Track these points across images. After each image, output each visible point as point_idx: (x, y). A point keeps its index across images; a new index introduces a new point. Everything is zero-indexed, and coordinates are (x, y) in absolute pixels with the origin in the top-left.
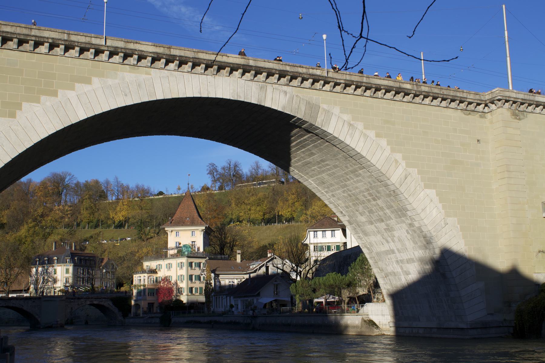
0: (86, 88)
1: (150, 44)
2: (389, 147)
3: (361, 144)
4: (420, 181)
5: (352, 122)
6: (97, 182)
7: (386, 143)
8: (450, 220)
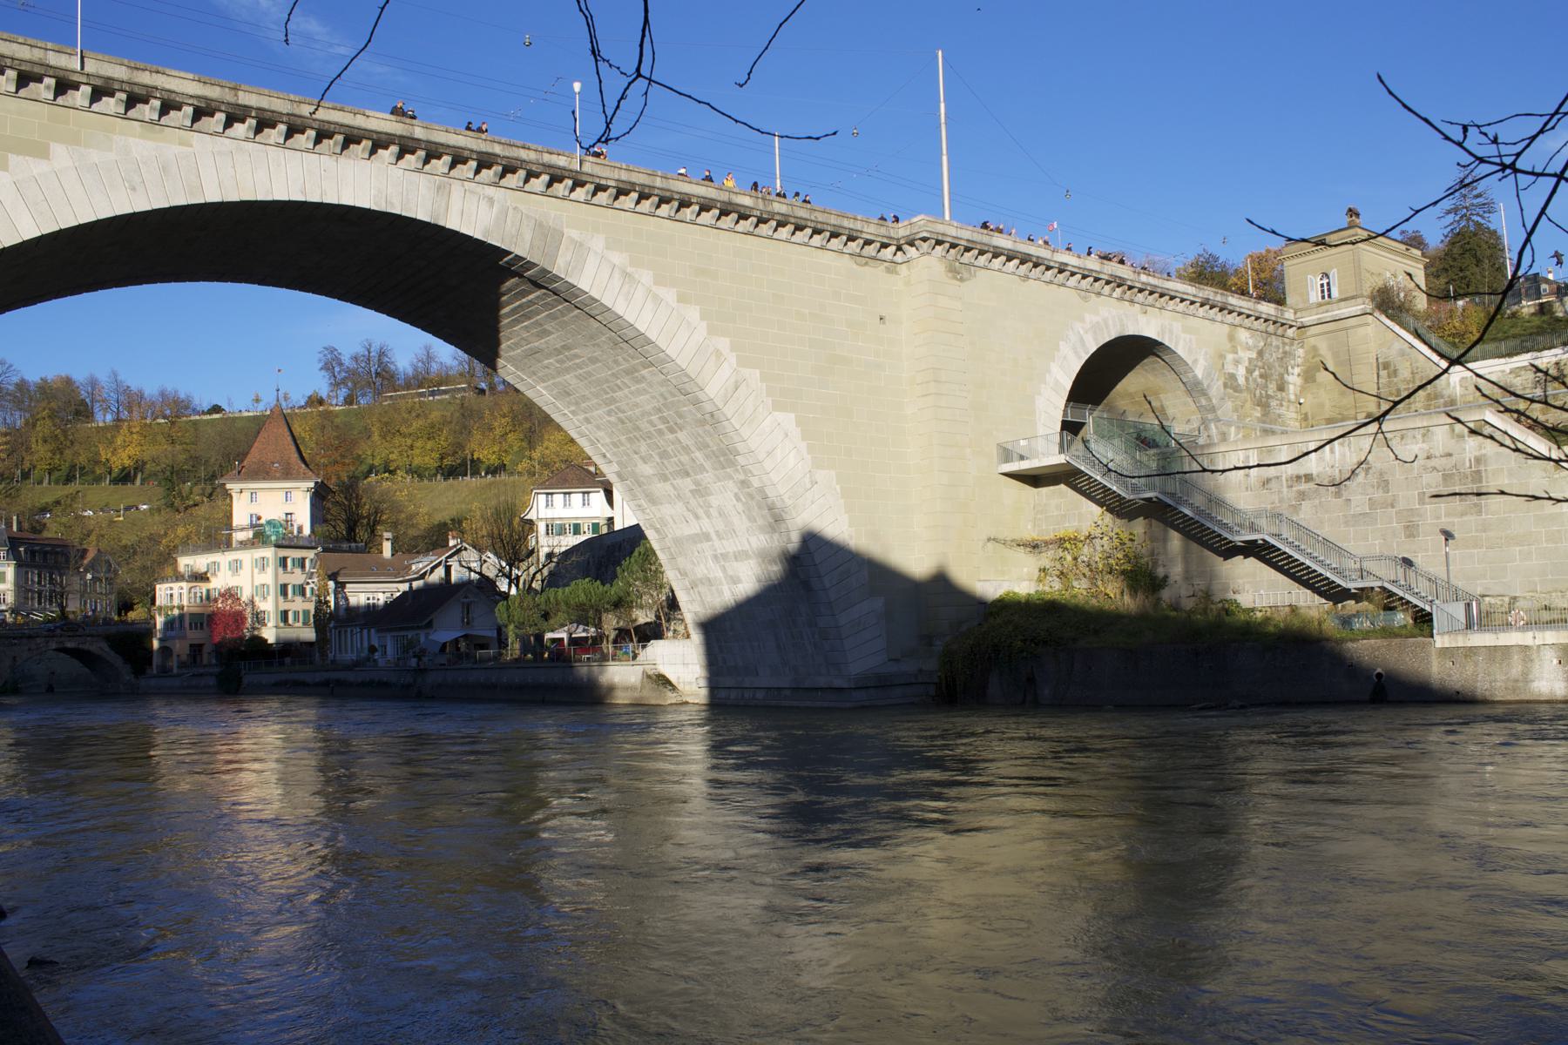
0: (37, 167)
1: (191, 76)
2: (704, 324)
5: (629, 270)
6: (68, 381)
7: (697, 315)
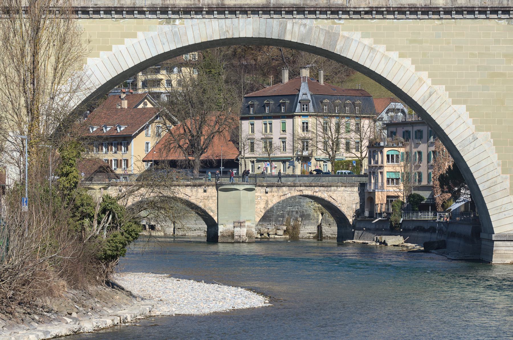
0: (134, 41)
2: (414, 66)
4: (448, 97)
5: (373, 46)
8: (481, 135)
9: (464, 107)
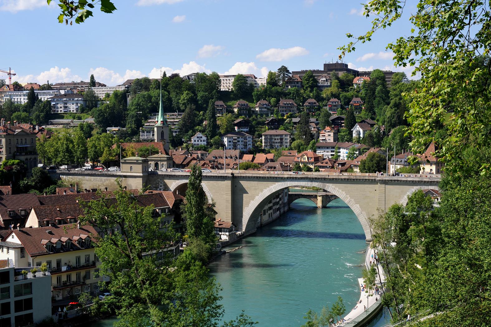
3: (337, 194)
9: (358, 205)
